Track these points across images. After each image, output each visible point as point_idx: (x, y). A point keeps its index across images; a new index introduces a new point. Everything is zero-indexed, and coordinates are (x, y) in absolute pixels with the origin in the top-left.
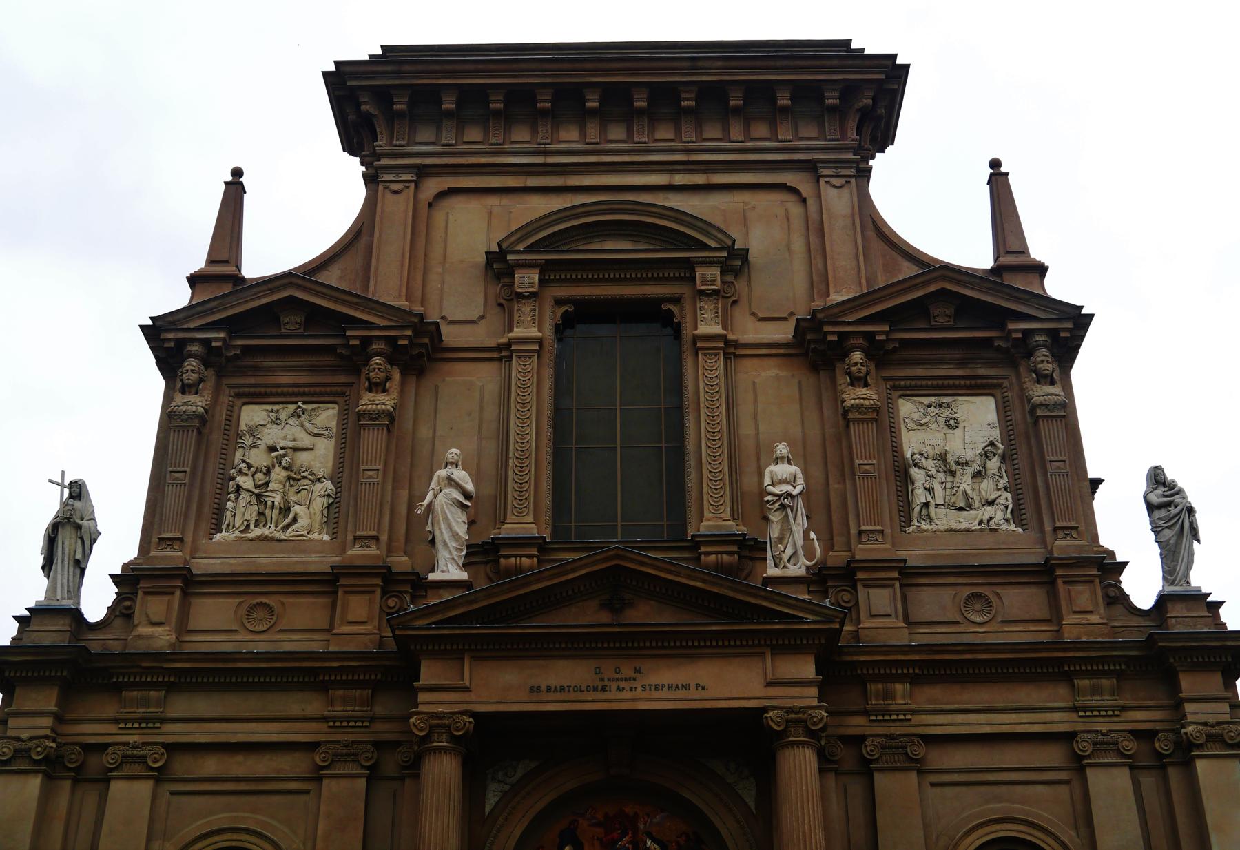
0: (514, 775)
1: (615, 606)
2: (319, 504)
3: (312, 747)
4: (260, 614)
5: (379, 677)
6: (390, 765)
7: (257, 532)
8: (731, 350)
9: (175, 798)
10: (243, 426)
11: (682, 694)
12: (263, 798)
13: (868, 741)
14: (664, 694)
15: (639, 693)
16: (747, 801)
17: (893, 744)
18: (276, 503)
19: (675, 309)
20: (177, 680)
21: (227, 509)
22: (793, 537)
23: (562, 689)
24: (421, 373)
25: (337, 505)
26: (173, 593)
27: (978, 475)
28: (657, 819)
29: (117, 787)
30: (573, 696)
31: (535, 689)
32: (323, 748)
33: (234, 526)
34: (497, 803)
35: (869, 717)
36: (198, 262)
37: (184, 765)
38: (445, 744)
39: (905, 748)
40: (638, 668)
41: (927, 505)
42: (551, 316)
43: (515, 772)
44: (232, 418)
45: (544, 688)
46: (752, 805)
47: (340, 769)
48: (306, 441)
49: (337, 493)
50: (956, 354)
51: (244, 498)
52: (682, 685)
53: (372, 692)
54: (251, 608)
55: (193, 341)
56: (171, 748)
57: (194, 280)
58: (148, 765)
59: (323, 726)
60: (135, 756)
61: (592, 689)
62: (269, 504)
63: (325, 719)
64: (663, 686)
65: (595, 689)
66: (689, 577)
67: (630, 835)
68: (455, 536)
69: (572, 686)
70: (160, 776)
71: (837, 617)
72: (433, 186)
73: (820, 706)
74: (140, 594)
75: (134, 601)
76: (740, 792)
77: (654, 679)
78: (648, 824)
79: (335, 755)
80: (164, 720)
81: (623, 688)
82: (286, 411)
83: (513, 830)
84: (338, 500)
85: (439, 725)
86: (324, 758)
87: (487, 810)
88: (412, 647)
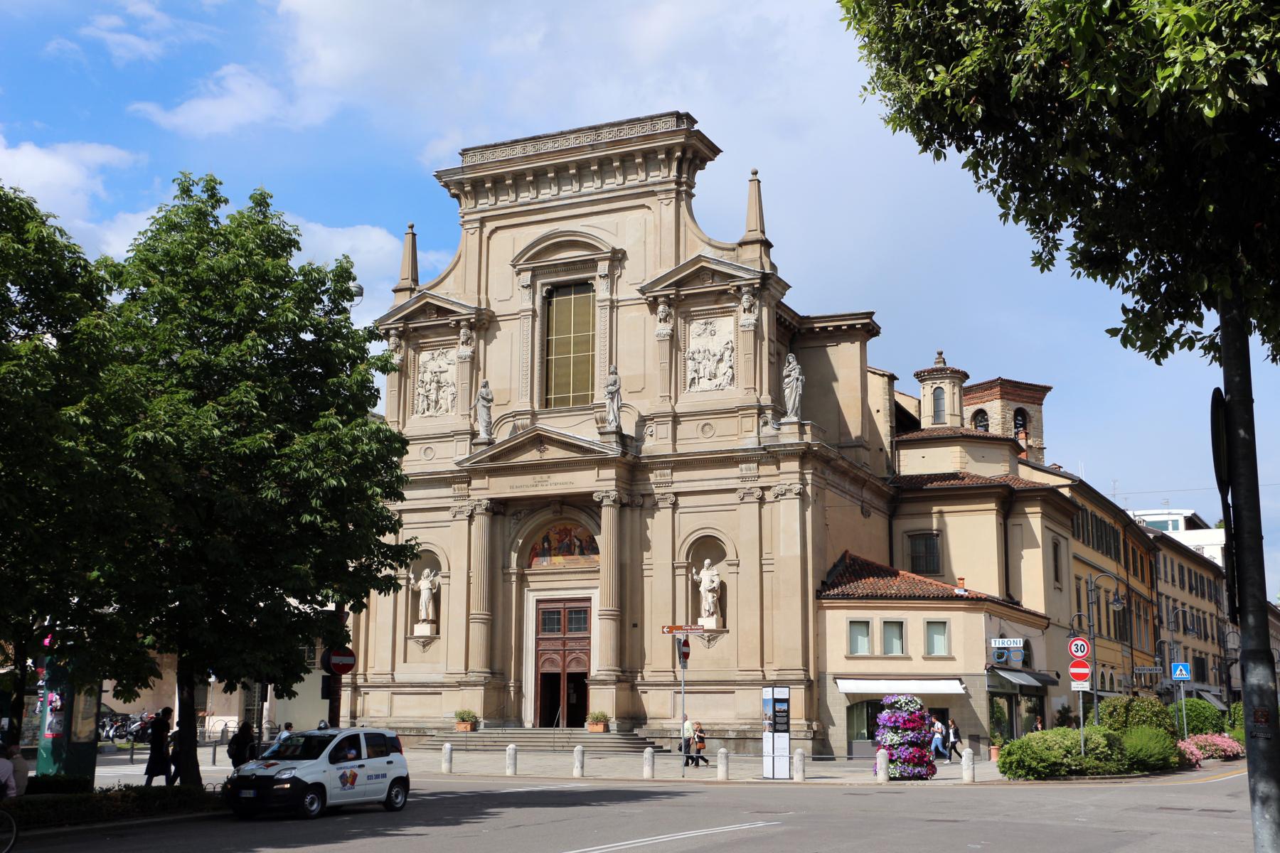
4: (429, 451)
10: (420, 363)
11: (565, 486)
19: (593, 282)
28: (579, 530)
42: (540, 293)
48: (445, 367)
50: (713, 298)
51: (421, 397)
55: (392, 329)
72: (490, 226)
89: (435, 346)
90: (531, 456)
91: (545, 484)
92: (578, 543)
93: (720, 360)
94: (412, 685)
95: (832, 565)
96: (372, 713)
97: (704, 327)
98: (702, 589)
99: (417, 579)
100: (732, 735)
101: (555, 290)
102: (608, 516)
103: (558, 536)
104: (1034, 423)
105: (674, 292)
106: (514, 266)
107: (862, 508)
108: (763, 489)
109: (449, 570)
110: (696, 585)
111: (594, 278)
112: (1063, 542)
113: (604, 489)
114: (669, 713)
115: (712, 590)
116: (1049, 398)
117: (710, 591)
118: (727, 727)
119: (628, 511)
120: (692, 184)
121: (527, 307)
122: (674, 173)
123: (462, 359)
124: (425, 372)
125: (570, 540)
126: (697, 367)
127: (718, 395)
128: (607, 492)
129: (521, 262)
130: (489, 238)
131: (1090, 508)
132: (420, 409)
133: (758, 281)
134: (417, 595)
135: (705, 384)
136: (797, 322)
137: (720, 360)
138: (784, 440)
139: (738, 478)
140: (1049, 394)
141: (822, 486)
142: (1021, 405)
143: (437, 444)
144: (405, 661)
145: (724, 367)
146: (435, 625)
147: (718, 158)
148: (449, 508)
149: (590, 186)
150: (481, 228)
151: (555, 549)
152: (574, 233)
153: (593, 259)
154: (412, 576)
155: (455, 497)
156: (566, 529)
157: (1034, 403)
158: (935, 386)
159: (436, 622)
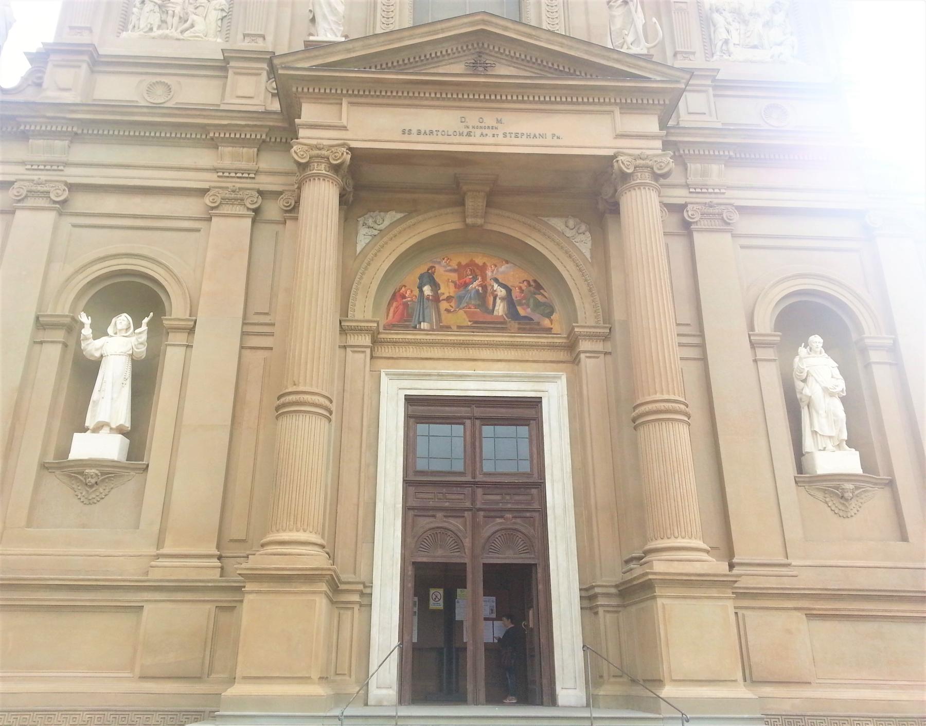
0: (382, 224)
2: (214, 16)
3: (203, 192)
5: (264, 137)
6: (273, 210)
7: (157, 33)
9: (77, 230)
12: (158, 234)
13: (690, 207)
15: (500, 139)
16: (584, 252)
17: (711, 210)
18: (176, 12)
20: (80, 132)
21: (133, 13)
22: (635, 26)
23: (431, 132)
25: (230, 17)
27: (767, 24)
29: (19, 214)
30: (440, 138)
31: (407, 132)
32: (211, 193)
33: (139, 28)
34: (367, 244)
35: (689, 189)
38: (324, 172)
39: (721, 214)
40: (499, 119)
41: (726, 42)
43: (383, 220)
45: (414, 131)
46: (588, 256)
47: (226, 210)
49: (229, 9)
52: (540, 135)
53: (258, 150)
54: (151, 85)
56: (73, 188)
58: (51, 199)
59: (214, 176)
60: (39, 192)
61: (458, 134)
62: (170, 12)
63: (215, 170)
64: (523, 134)
65: (461, 134)
66: (548, 41)
67: (480, 280)
68: (333, 10)
69: (441, 130)
70: (61, 208)
71: (683, 78)
73: (664, 154)
74: (50, 66)
75: (44, 73)
76: (577, 244)
77: (514, 129)
78: (495, 273)
80: (66, 164)
81: (487, 135)
83: (382, 264)
84: (230, 13)
85: (318, 154)
86: (213, 200)
87: (359, 249)
88: (294, 89)
91: (489, 132)
92: (501, 292)
99: (100, 331)
103: (454, 276)
151: (449, 299)
154: (85, 319)
156: (472, 265)
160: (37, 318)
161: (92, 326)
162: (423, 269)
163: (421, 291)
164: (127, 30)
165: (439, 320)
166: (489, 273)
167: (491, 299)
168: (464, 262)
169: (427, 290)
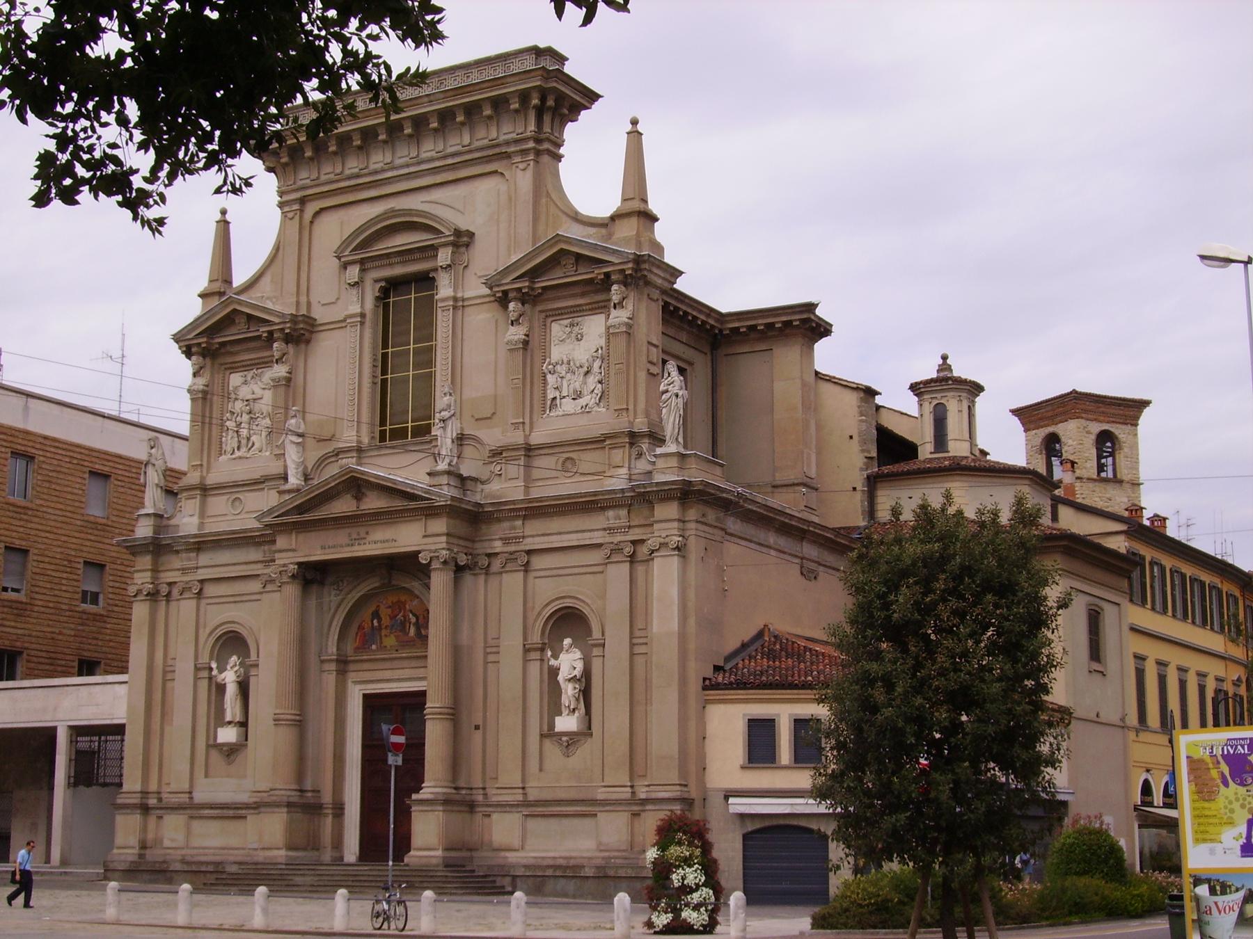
1: (358, 498)
4: (237, 503)
7: (237, 454)
8: (458, 304)
10: (231, 388)
11: (386, 545)
14: (379, 545)
24: (308, 342)
26: (196, 498)
36: (203, 284)
37: (210, 590)
41: (555, 398)
42: (371, 292)
44: (225, 384)
48: (259, 392)
51: (230, 432)
57: (203, 296)
65: (349, 545)
72: (311, 208)
79: (266, 581)
80: (197, 568)
82: (250, 374)
89: (248, 365)
90: (343, 506)
91: (362, 542)
92: (413, 620)
93: (587, 373)
94: (212, 806)
95: (738, 644)
96: (167, 843)
97: (568, 329)
98: (560, 678)
99: (222, 669)
100: (589, 872)
101: (391, 287)
102: (440, 581)
103: (389, 611)
104: (1126, 450)
105: (527, 284)
106: (339, 258)
107: (802, 567)
108: (634, 542)
109: (258, 657)
110: (554, 672)
111: (435, 270)
112: (1109, 613)
113: (433, 547)
114: (516, 843)
115: (573, 679)
116: (1146, 417)
117: (569, 680)
118: (585, 862)
119: (468, 578)
120: (559, 141)
121: (355, 312)
122: (532, 127)
123: (276, 384)
124: (236, 399)
125: (404, 616)
126: (559, 384)
127: (583, 421)
128: (436, 551)
129: (347, 253)
130: (312, 222)
131: (1168, 562)
132: (229, 449)
133: (630, 265)
134: (221, 688)
135: (568, 406)
136: (717, 320)
137: (587, 373)
138: (659, 478)
139: (605, 529)
140: (1147, 412)
141: (719, 539)
142: (1106, 427)
143: (247, 494)
144: (206, 776)
145: (592, 381)
146: (244, 729)
147: (597, 106)
148: (258, 575)
149: (429, 148)
150: (302, 211)
151: (386, 627)
152: (409, 212)
153: (432, 245)
154: (214, 665)
155: (266, 562)
156: (399, 601)
157: (1126, 424)
158: (935, 402)
159: (244, 724)
160: (195, 665)
161: (217, 668)
162: (373, 608)
163: (373, 624)
164: (221, 455)
165: (381, 643)
166: (407, 606)
167: (408, 625)
168: (394, 601)
169: (375, 621)
